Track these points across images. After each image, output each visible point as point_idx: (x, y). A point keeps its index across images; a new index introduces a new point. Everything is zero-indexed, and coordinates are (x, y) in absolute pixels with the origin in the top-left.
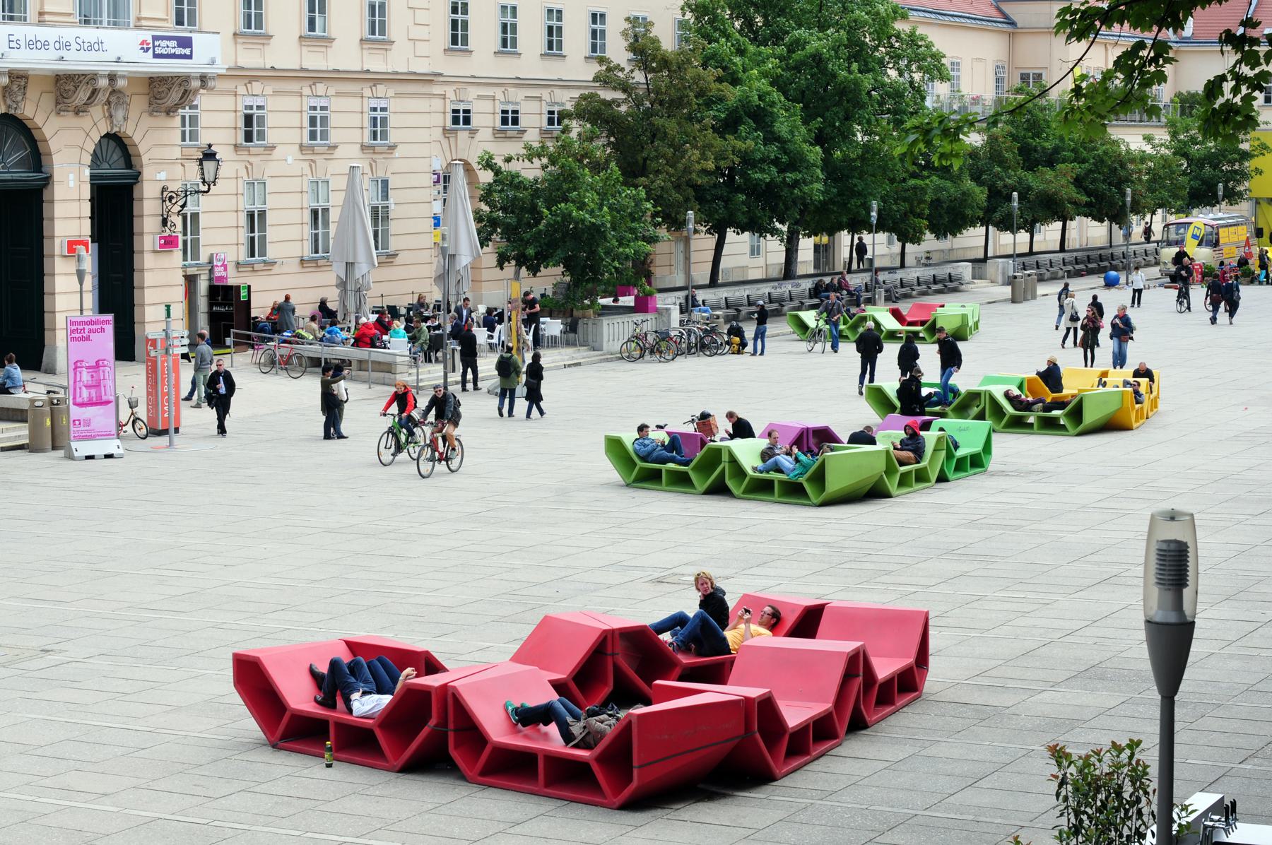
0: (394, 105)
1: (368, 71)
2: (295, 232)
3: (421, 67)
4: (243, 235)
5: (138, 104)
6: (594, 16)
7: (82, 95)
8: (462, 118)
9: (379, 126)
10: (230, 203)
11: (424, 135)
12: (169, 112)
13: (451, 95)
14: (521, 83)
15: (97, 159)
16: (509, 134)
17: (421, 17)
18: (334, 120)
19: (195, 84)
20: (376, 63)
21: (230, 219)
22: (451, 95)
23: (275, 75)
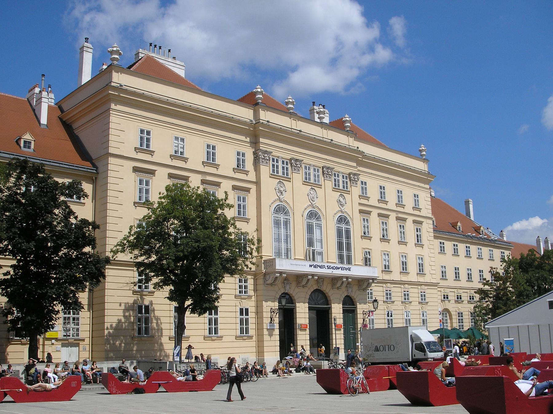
0: (427, 291)
1: (419, 282)
3: (434, 281)
5: (355, 288)
8: (446, 297)
9: (423, 296)
11: (436, 300)
16: (459, 302)
17: (433, 268)
18: (410, 295)
20: (421, 279)
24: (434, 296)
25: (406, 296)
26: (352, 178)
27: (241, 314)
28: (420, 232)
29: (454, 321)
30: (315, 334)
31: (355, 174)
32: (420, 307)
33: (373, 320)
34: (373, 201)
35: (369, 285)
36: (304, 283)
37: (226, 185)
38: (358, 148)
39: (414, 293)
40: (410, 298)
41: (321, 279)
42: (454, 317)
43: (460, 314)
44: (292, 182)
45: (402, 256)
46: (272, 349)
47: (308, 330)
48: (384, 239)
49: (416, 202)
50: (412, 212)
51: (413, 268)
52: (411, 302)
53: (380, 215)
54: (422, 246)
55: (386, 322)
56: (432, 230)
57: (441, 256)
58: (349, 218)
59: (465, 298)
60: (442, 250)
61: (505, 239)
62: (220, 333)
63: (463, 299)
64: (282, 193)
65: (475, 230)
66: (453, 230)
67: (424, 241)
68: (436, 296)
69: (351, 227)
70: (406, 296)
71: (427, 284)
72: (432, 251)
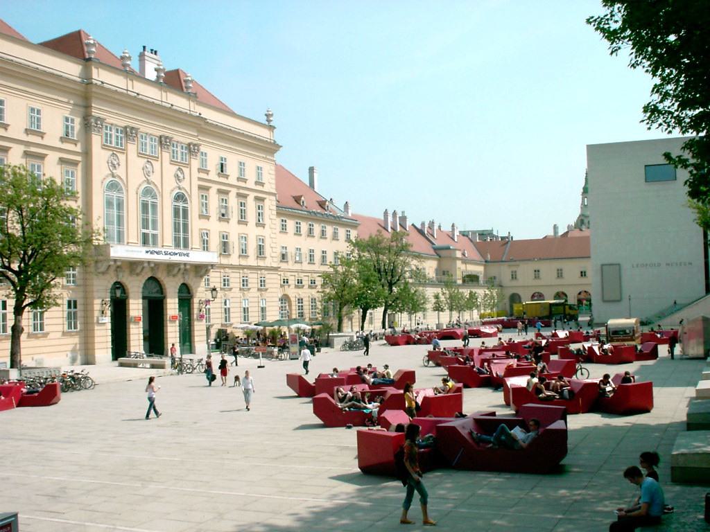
0: (267, 276)
2: (238, 315)
3: (275, 265)
4: (224, 316)
5: (192, 274)
6: (323, 252)
7: (176, 270)
8: (286, 281)
9: (263, 283)
10: (219, 305)
11: (276, 286)
12: (201, 277)
13: (282, 275)
14: (303, 272)
15: (180, 291)
18: (250, 281)
19: (210, 267)
20: (261, 263)
21: (219, 310)
22: (282, 275)
23: (232, 267)
24: (273, 280)
25: (245, 282)
26: (192, 149)
27: (69, 307)
28: (244, 207)
29: (294, 308)
30: (147, 328)
31: (195, 145)
32: (259, 294)
33: (209, 309)
34: (232, 180)
35: (207, 271)
36: (138, 270)
37: (53, 157)
38: (200, 114)
39: (253, 279)
40: (230, 284)
41: (157, 265)
42: (293, 303)
43: (300, 301)
44: (159, 162)
45: (242, 237)
46: (104, 345)
47: (141, 323)
48: (223, 217)
49: (259, 175)
50: (254, 187)
51: (252, 251)
52: (249, 289)
53: (257, 199)
54: (263, 226)
55: (223, 311)
56: (275, 208)
57: (283, 236)
58: (186, 195)
59: (306, 282)
60: (284, 229)
61: (350, 215)
62: (46, 329)
63: (304, 283)
64: (115, 167)
65: (320, 205)
66: (296, 206)
67: (267, 221)
68: (275, 281)
69: (158, 201)
70: (245, 282)
71: (267, 269)
72: (274, 231)
